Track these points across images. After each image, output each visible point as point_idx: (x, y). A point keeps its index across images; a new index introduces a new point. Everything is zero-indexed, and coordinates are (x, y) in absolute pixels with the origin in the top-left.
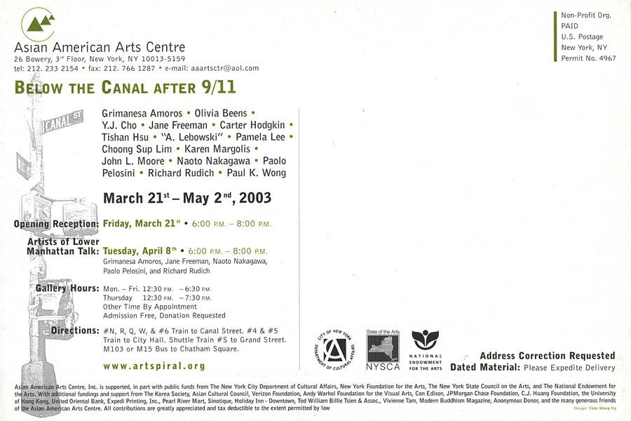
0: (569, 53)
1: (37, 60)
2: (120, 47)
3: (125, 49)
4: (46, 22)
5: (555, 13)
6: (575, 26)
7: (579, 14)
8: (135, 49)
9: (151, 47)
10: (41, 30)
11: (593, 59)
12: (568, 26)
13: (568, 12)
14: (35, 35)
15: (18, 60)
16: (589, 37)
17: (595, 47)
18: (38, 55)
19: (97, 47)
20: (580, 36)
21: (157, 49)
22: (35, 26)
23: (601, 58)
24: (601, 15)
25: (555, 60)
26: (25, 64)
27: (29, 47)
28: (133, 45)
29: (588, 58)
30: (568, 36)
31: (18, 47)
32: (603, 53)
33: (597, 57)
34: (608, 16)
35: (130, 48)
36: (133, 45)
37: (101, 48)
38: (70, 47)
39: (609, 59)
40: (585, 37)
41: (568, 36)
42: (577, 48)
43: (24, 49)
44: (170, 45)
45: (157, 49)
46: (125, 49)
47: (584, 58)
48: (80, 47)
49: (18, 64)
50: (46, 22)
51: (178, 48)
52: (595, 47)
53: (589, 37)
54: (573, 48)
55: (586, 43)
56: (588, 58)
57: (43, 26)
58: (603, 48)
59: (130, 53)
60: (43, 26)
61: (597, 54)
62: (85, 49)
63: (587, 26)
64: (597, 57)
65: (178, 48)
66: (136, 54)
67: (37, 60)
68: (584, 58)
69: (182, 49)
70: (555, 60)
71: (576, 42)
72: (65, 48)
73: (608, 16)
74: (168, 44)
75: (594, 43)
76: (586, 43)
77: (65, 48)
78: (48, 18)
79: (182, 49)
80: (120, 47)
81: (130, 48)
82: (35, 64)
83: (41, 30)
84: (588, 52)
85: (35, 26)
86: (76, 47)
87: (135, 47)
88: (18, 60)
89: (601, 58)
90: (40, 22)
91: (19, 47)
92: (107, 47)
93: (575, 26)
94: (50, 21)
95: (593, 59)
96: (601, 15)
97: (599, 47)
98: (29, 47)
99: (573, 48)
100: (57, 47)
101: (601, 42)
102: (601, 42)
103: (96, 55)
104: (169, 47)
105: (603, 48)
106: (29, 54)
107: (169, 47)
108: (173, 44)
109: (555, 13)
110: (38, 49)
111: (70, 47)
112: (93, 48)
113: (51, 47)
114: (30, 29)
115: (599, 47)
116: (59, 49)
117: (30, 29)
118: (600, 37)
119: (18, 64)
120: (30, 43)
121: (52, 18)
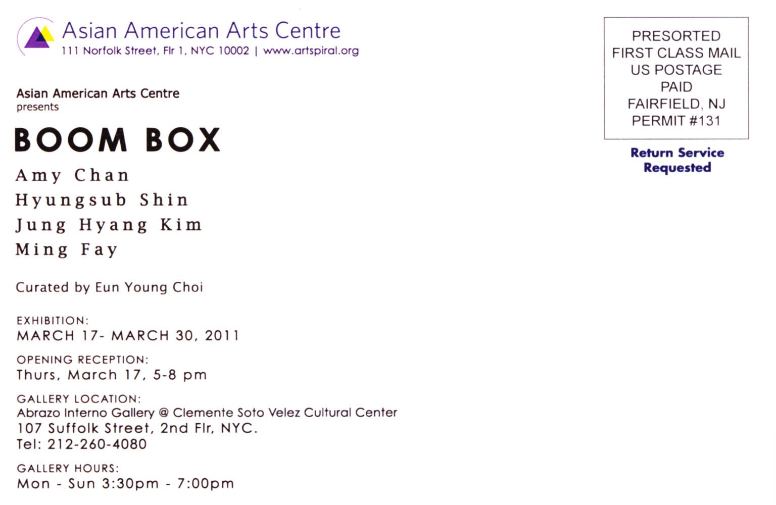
9: (285, 30)
21: (295, 35)
28: (254, 27)
35: (249, 32)
37: (203, 33)
38: (153, 31)
43: (78, 34)
44: (317, 27)
45: (295, 35)
48: (171, 30)
51: (328, 32)
65: (328, 32)
69: (335, 35)
72: (146, 31)
77: (146, 31)
79: (335, 35)
81: (249, 32)
87: (257, 31)
103: (197, 43)
104: (314, 30)
108: (321, 25)
111: (153, 31)
112: (191, 33)
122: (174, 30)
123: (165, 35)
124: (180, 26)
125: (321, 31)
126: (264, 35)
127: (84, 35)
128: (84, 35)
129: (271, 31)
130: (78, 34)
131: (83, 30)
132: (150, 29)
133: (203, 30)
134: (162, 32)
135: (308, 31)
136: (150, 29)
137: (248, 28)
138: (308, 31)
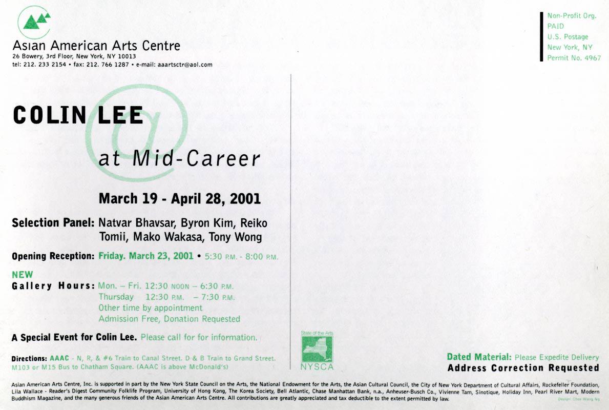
0: (554, 53)
1: (31, 57)
2: (116, 45)
3: (121, 47)
4: (42, 19)
5: (542, 14)
6: (561, 26)
7: (565, 14)
8: (131, 47)
9: (147, 45)
10: (37, 28)
11: (578, 59)
12: (554, 26)
13: (554, 12)
15: (15, 57)
16: (576, 37)
17: (580, 47)
18: (36, 52)
19: (94, 45)
20: (566, 36)
21: (153, 48)
22: (31, 24)
23: (587, 58)
24: (586, 16)
25: (542, 60)
26: (22, 61)
27: (27, 45)
29: (574, 58)
30: (554, 36)
31: (17, 45)
32: (588, 53)
33: (582, 57)
34: (593, 17)
36: (129, 44)
37: (98, 47)
38: (67, 46)
39: (593, 58)
40: (570, 37)
41: (554, 36)
42: (563, 48)
43: (22, 47)
44: (166, 44)
46: (121, 47)
47: (570, 58)
48: (78, 45)
49: (16, 61)
50: (42, 19)
51: (173, 47)
52: (580, 47)
53: (576, 37)
54: (559, 48)
55: (571, 43)
56: (574, 58)
58: (588, 47)
59: (126, 51)
60: (38, 24)
61: (583, 54)
62: (82, 47)
63: (572, 27)
64: (582, 57)
65: (173, 47)
66: (132, 52)
67: (31, 57)
68: (570, 58)
70: (542, 60)
71: (561, 42)
72: (63, 46)
73: (593, 17)
74: (164, 43)
75: (579, 43)
76: (571, 43)
77: (63, 46)
78: (44, 15)
79: (177, 48)
80: (117, 45)
82: (31, 60)
83: (37, 28)
84: (573, 52)
85: (31, 24)
86: (74, 45)
87: (131, 46)
88: (15, 57)
89: (587, 58)
90: (36, 20)
91: (17, 45)
92: (104, 46)
93: (561, 26)
94: (46, 19)
95: (578, 59)
96: (586, 16)
97: (585, 47)
98: (27, 45)
99: (559, 48)
100: (55, 45)
101: (585, 42)
102: (585, 42)
103: (93, 52)
104: (164, 46)
105: (588, 47)
106: (28, 52)
107: (164, 46)
108: (169, 43)
109: (542, 14)
110: (36, 47)
111: (67, 46)
112: (91, 46)
113: (49, 45)
114: (24, 28)
115: (585, 47)
116: (57, 47)
117: (24, 28)
118: (585, 37)
119: (16, 61)
121: (48, 16)
122: (79, 46)
123: (74, 48)
125: (168, 47)
126: (135, 48)
127: (25, 48)
128: (25, 48)
129: (139, 46)
130: (22, 47)
131: (25, 45)
132: (65, 45)
133: (97, 45)
134: (73, 46)
135: (160, 46)
136: (65, 45)
137: (126, 44)
138: (160, 46)
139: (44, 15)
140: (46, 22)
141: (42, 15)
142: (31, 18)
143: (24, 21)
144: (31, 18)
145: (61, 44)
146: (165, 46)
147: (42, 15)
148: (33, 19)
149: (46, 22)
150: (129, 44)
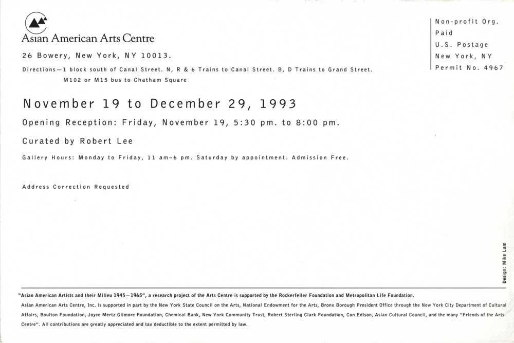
9: (128, 38)
10: (38, 27)
14: (34, 30)
22: (34, 24)
35: (112, 39)
38: (66, 39)
50: (42, 22)
57: (39, 25)
60: (39, 25)
62: (77, 39)
72: (63, 39)
77: (63, 39)
78: (43, 19)
81: (112, 39)
83: (38, 27)
85: (34, 24)
90: (38, 22)
94: (45, 21)
111: (66, 39)
114: (30, 27)
117: (30, 27)
120: (34, 36)
124: (78, 36)
129: (121, 39)
132: (64, 38)
136: (64, 38)
139: (43, 19)
140: (44, 23)
141: (42, 18)
142: (34, 21)
143: (29, 22)
144: (34, 21)
145: (61, 38)
146: (142, 39)
147: (42, 18)
148: (36, 22)
149: (44, 23)
150: (114, 37)
